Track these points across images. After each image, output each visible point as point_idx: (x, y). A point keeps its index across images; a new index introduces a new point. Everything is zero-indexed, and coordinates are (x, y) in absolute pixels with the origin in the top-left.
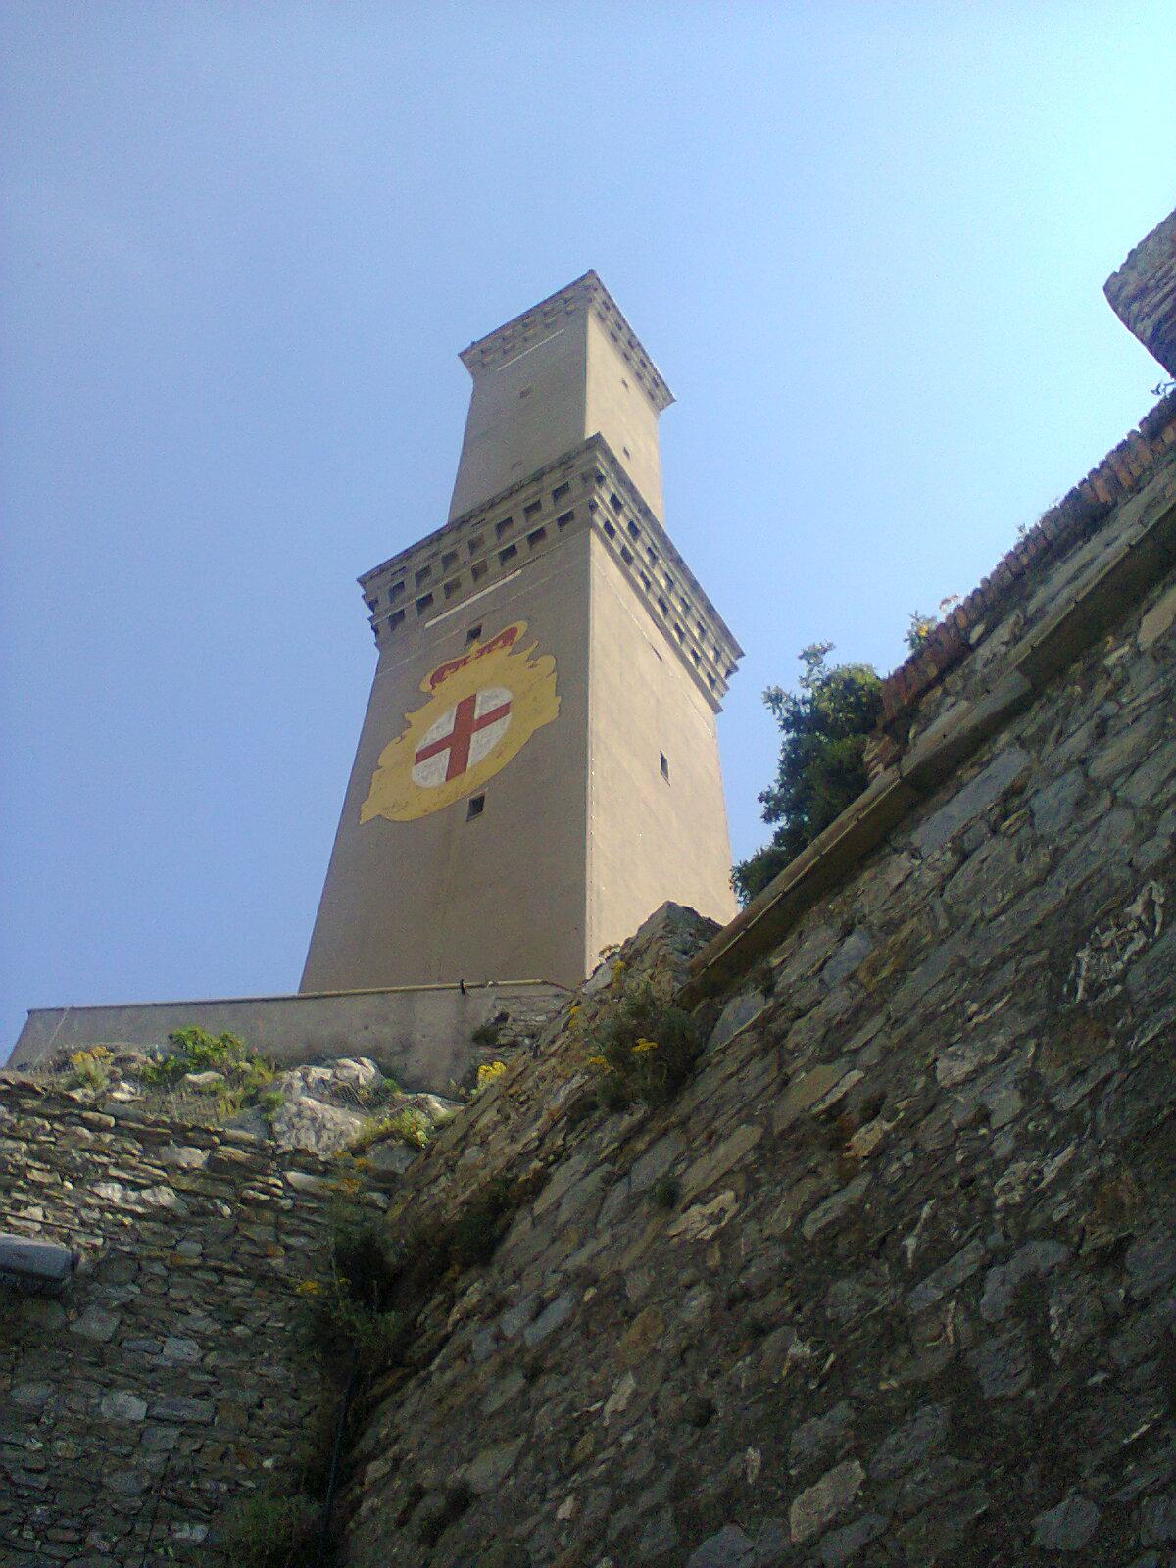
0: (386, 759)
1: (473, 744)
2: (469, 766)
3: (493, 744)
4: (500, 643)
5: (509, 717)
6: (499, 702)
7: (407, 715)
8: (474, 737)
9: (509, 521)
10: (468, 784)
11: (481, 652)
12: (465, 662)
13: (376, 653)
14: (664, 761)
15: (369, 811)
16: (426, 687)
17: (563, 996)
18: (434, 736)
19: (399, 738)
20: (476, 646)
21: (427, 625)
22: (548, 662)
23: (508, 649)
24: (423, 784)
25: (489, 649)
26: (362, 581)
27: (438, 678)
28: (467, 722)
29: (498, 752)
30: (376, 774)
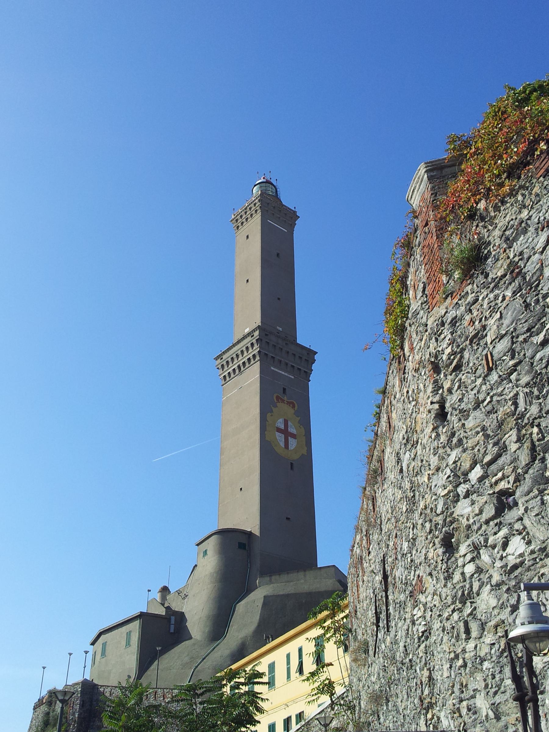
3: (294, 447)
16: (275, 399)
21: (272, 368)
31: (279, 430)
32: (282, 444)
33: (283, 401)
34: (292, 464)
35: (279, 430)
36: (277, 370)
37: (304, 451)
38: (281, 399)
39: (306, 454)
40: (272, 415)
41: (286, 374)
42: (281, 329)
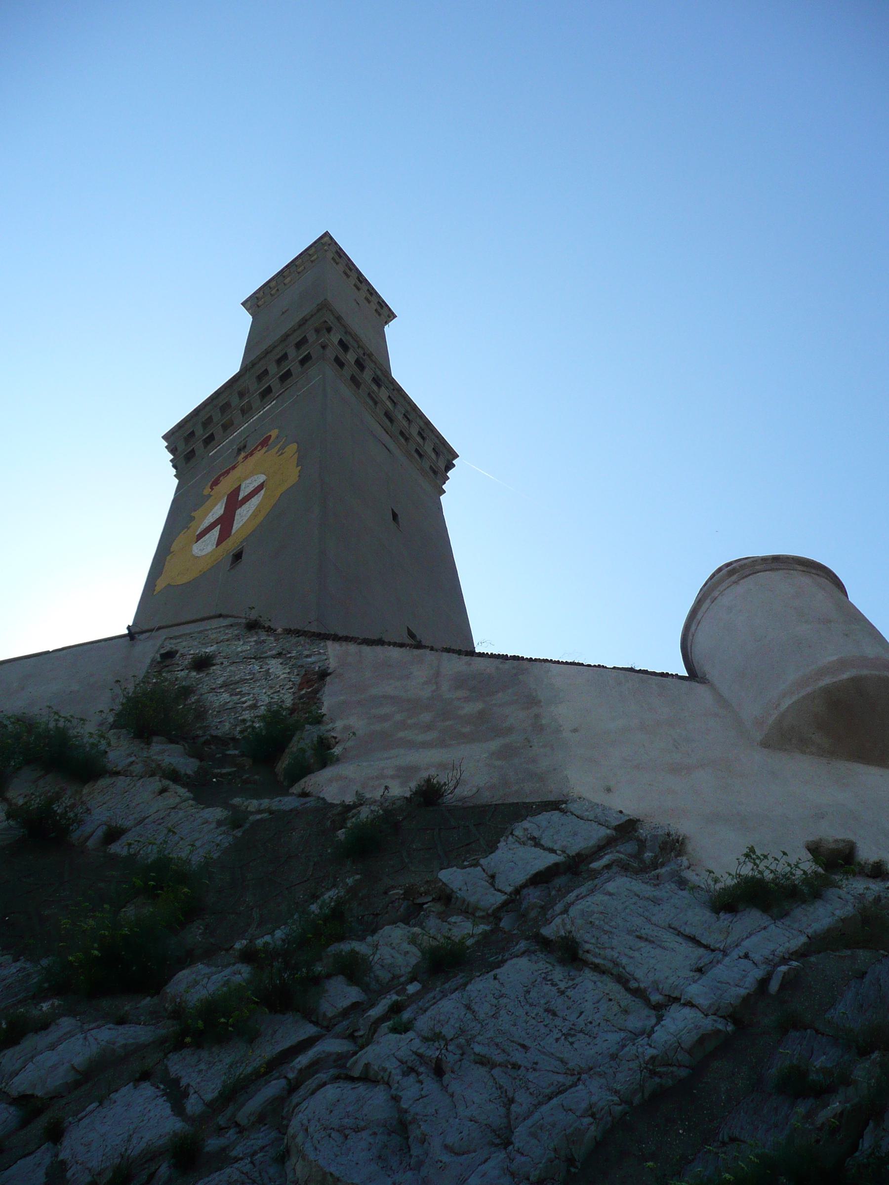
0: (175, 547)
1: (237, 517)
2: (233, 531)
3: (251, 512)
4: (259, 448)
5: (263, 492)
6: (256, 484)
8: (238, 511)
10: (231, 545)
11: (246, 457)
12: (234, 468)
13: (176, 481)
14: (395, 516)
15: (161, 584)
16: (207, 491)
17: (238, 624)
23: (265, 449)
24: (200, 554)
25: (251, 454)
26: (165, 437)
27: (216, 483)
28: (234, 502)
29: (255, 515)
30: (168, 558)
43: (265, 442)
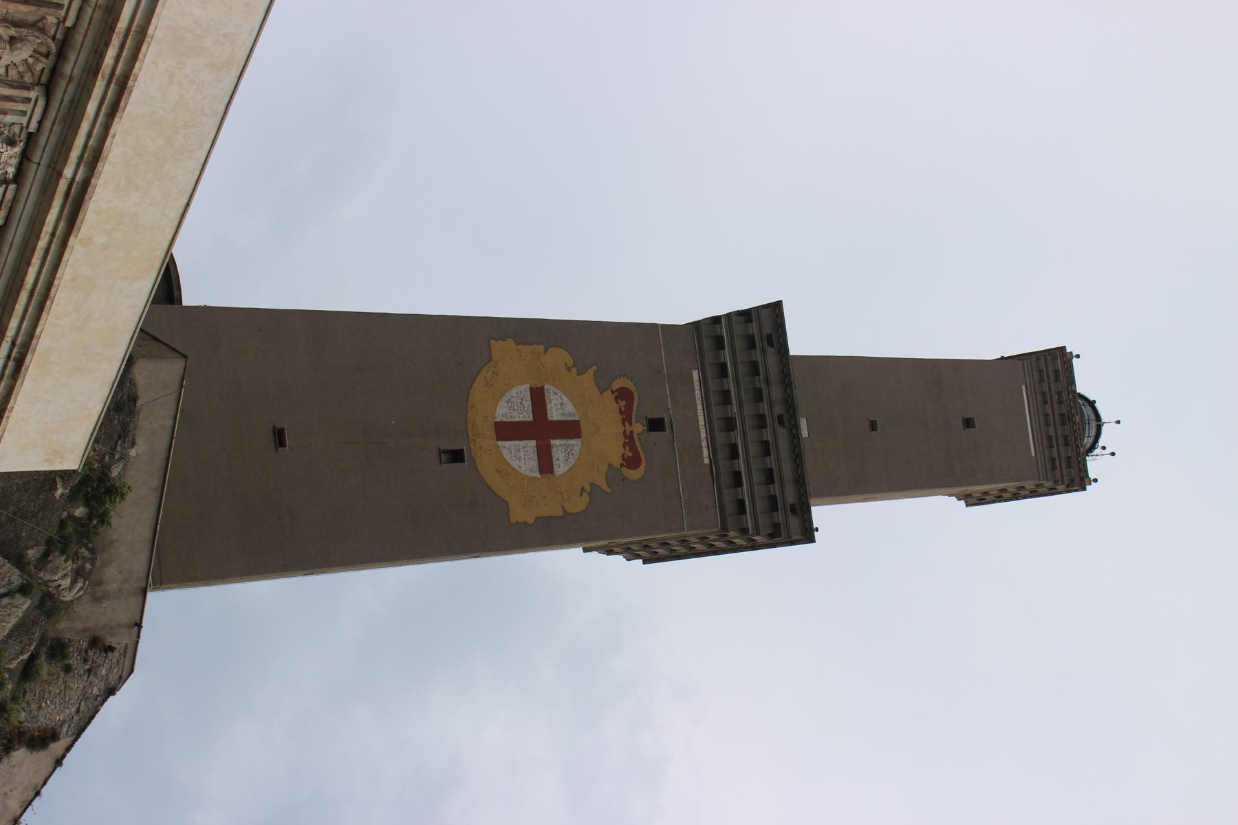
1: (523, 443)
2: (500, 443)
3: (515, 463)
4: (630, 454)
7: (595, 368)
9: (767, 453)
16: (618, 384)
18: (554, 402)
19: (570, 362)
20: (638, 428)
21: (695, 374)
22: (579, 504)
23: (616, 461)
29: (505, 471)
31: (538, 397)
32: (504, 412)
33: (626, 416)
34: (457, 456)
35: (538, 397)
36: (697, 392)
37: (520, 514)
38: (629, 408)
39: (513, 521)
40: (569, 369)
41: (703, 435)
42: (805, 433)
43: (632, 462)
